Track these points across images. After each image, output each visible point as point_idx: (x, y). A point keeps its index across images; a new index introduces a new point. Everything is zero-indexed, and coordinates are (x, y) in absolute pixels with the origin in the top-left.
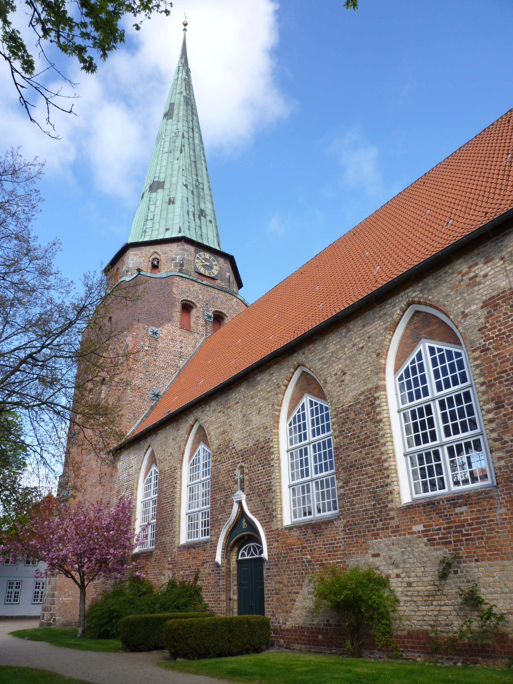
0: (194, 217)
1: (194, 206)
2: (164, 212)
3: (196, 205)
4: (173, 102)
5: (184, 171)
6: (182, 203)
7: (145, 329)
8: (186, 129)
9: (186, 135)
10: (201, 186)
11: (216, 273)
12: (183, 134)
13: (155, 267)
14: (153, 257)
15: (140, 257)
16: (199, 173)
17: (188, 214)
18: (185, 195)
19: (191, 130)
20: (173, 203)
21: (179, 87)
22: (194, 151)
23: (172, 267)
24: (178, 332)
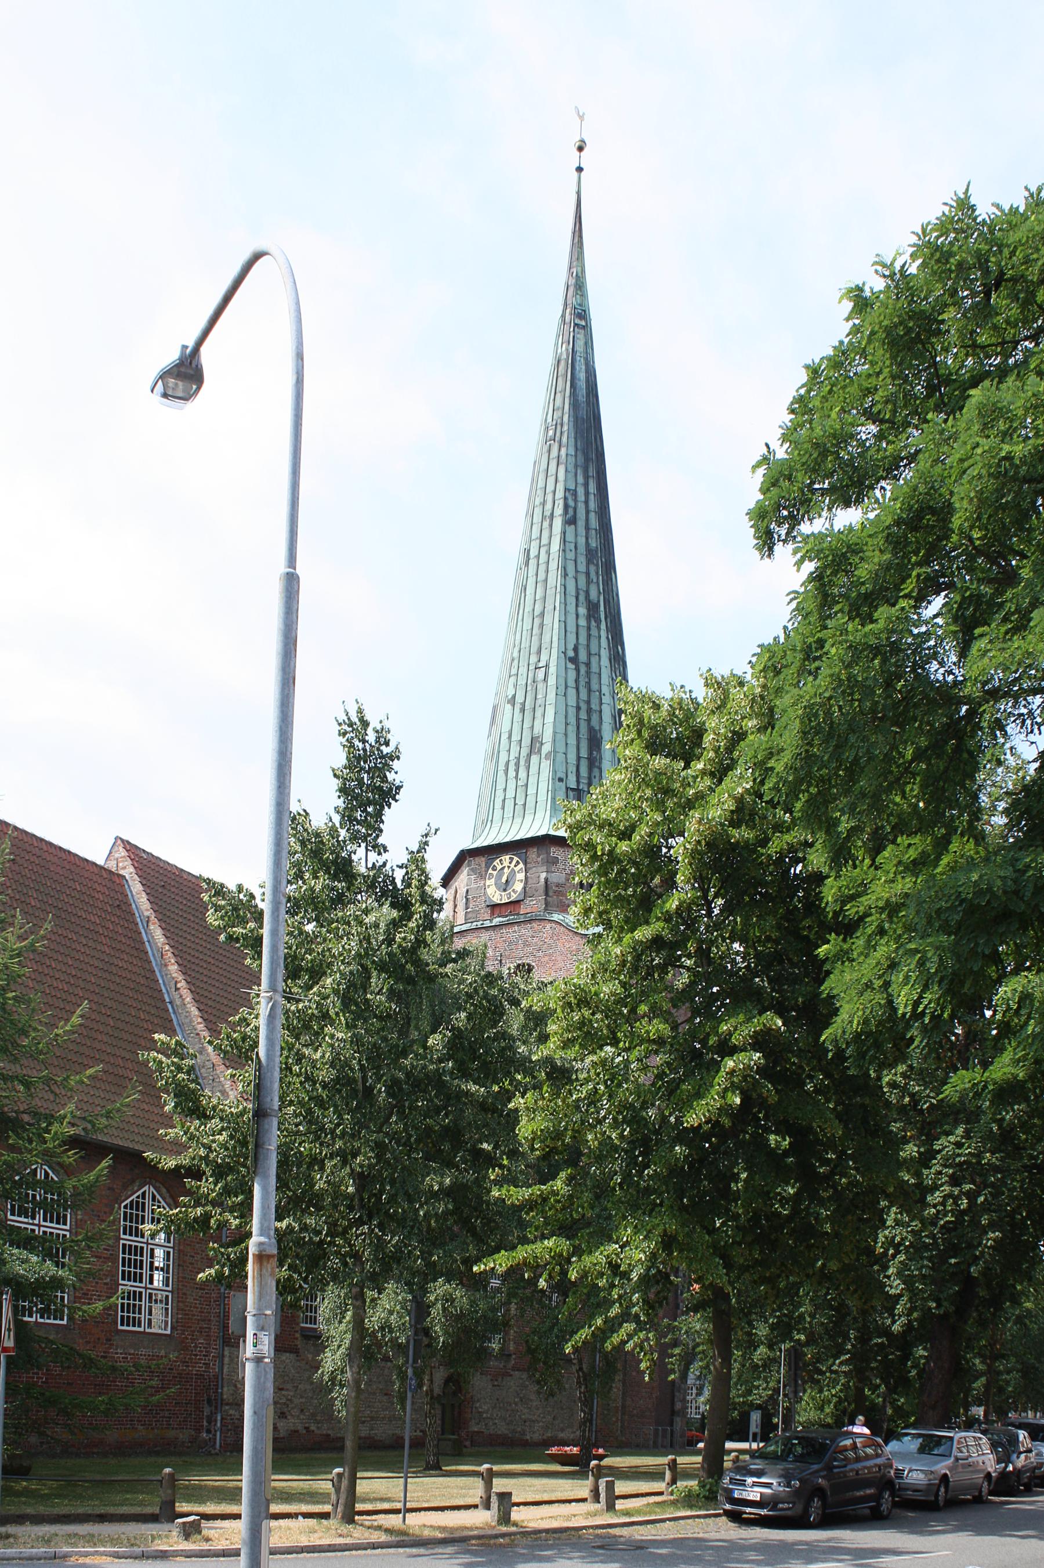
0: (517, 771)
9: (533, 553)
11: (519, 887)
19: (546, 524)
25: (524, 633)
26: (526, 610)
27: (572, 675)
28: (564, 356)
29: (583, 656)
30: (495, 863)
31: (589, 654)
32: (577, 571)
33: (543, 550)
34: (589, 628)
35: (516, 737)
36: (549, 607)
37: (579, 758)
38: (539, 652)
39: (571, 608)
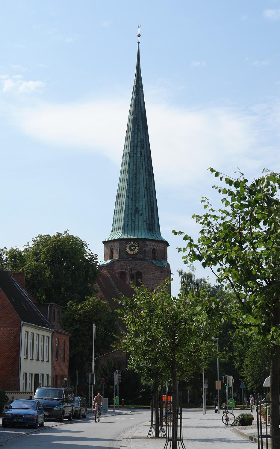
0: (131, 217)
3: (133, 207)
5: (128, 185)
11: (137, 251)
16: (138, 181)
17: (128, 216)
19: (135, 148)
26: (131, 172)
27: (146, 192)
28: (137, 98)
29: (148, 187)
31: (150, 186)
32: (145, 162)
33: (135, 155)
34: (149, 179)
35: (130, 207)
37: (149, 215)
38: (136, 184)
39: (144, 173)
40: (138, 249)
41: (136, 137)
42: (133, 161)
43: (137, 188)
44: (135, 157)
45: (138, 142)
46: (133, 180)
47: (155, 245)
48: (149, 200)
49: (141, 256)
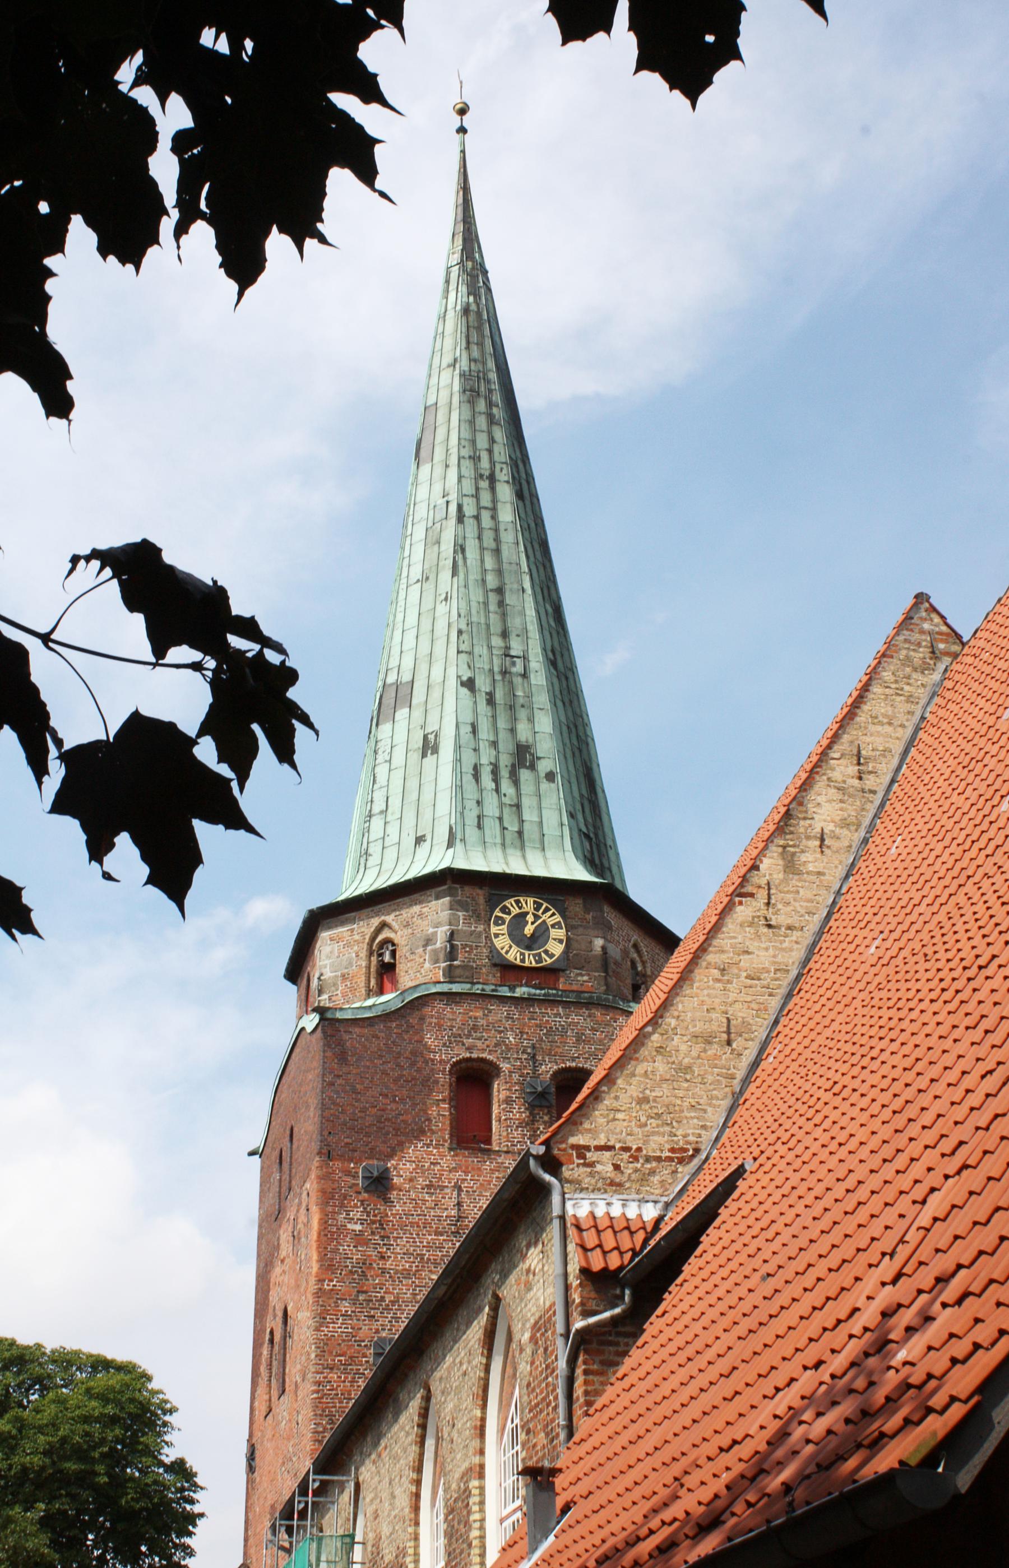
0: (496, 780)
1: (494, 744)
2: (413, 783)
3: (503, 735)
4: (431, 401)
5: (465, 637)
6: (458, 747)
7: (348, 1173)
8: (468, 487)
9: (469, 510)
10: (519, 668)
11: (557, 949)
12: (460, 507)
13: (385, 972)
14: (380, 938)
15: (348, 945)
16: (515, 623)
17: (476, 776)
18: (467, 717)
19: (484, 484)
20: (435, 750)
21: (449, 342)
22: (497, 551)
23: (427, 965)
24: (448, 1160)
25: (474, 604)
28: (473, 307)
30: (507, 903)
33: (486, 515)
35: (485, 733)
36: (511, 585)
38: (505, 635)
40: (561, 941)
41: (482, 442)
42: (480, 538)
43: (513, 653)
44: (486, 521)
45: (498, 467)
46: (487, 617)
47: (635, 946)
48: (572, 726)
49: (583, 980)
